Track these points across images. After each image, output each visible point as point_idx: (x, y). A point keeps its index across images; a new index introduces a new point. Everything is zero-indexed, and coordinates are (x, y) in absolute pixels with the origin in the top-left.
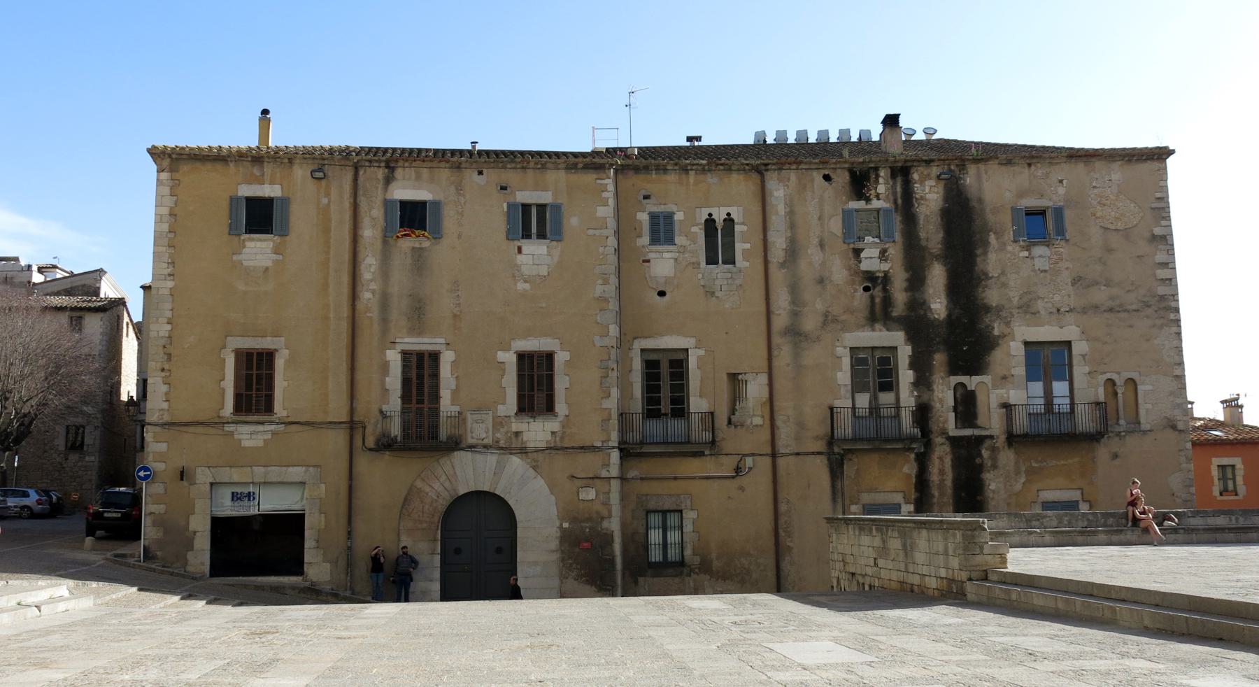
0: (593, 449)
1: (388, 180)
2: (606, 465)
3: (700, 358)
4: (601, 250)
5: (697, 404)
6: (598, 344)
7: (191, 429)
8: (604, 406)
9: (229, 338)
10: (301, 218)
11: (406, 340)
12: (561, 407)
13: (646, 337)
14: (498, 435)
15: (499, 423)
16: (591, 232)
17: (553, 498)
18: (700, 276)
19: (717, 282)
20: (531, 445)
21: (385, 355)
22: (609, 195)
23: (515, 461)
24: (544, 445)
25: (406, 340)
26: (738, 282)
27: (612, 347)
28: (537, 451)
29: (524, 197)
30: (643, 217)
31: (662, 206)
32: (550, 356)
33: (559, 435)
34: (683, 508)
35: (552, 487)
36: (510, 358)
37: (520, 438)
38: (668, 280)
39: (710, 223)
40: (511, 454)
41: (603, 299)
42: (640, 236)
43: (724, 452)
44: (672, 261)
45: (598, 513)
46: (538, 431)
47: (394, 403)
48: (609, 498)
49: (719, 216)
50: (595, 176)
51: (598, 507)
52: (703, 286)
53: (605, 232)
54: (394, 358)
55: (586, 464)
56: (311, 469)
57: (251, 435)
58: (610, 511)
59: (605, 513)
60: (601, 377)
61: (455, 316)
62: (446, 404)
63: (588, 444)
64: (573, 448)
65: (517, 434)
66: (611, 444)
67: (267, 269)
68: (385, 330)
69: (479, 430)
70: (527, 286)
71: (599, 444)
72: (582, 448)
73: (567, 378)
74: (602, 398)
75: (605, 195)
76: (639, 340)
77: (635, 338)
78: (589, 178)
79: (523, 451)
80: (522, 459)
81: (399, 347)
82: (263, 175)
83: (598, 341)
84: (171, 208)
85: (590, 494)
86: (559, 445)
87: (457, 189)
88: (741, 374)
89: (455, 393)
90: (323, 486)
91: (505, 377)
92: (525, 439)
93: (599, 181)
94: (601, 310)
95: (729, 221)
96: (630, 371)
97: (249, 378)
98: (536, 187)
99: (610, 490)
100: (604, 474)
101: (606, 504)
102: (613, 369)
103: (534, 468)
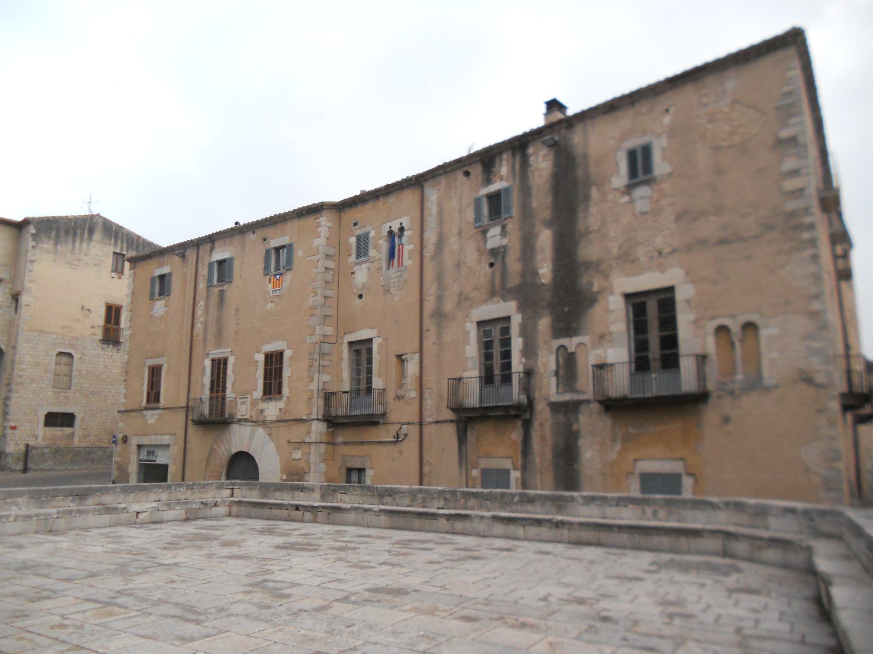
0: (301, 421)
1: (212, 249)
2: (309, 433)
3: (380, 344)
4: (314, 270)
5: (377, 383)
6: (308, 342)
7: (132, 414)
8: (309, 388)
9: (147, 360)
10: (176, 285)
11: (215, 351)
12: (285, 391)
13: (350, 332)
14: (252, 413)
15: (254, 403)
16: (309, 259)
17: (278, 457)
18: (382, 278)
19: (392, 281)
20: (269, 418)
21: (204, 362)
22: (324, 231)
23: (260, 431)
24: (275, 418)
25: (215, 351)
26: (404, 278)
27: (317, 343)
28: (272, 422)
29: (275, 243)
30: (353, 240)
31: (364, 228)
32: (281, 354)
33: (284, 410)
34: (366, 467)
35: (278, 448)
36: (260, 358)
37: (263, 414)
38: (364, 286)
39: (391, 233)
40: (258, 425)
41: (313, 307)
42: (350, 255)
43: (391, 421)
44: (367, 269)
45: (302, 469)
46: (272, 410)
47: (207, 394)
48: (309, 458)
49: (396, 228)
50: (314, 217)
51: (302, 464)
52: (383, 286)
53: (318, 257)
54: (208, 363)
55: (297, 432)
56: (172, 436)
57: (152, 417)
58: (309, 469)
59: (306, 470)
60: (309, 366)
61: (236, 332)
62: (230, 394)
63: (299, 417)
64: (291, 420)
65: (262, 411)
66: (313, 417)
67: (162, 317)
68: (205, 346)
69: (243, 410)
70: (272, 305)
71: (305, 417)
72: (295, 420)
73: (290, 369)
74: (309, 382)
75: (319, 229)
76: (347, 335)
77: (345, 334)
78: (309, 221)
79: (264, 423)
80: (263, 429)
81: (211, 357)
82: (164, 261)
83: (309, 340)
84: (133, 290)
85: (298, 455)
86: (284, 418)
87: (242, 247)
88: (403, 355)
89: (233, 384)
90: (176, 447)
91: (258, 371)
92: (266, 414)
93: (317, 221)
94: (312, 316)
95: (402, 229)
96: (342, 359)
97: (153, 381)
98: (283, 234)
99: (310, 452)
100: (307, 440)
101: (307, 462)
102: (316, 360)
103: (270, 435)
